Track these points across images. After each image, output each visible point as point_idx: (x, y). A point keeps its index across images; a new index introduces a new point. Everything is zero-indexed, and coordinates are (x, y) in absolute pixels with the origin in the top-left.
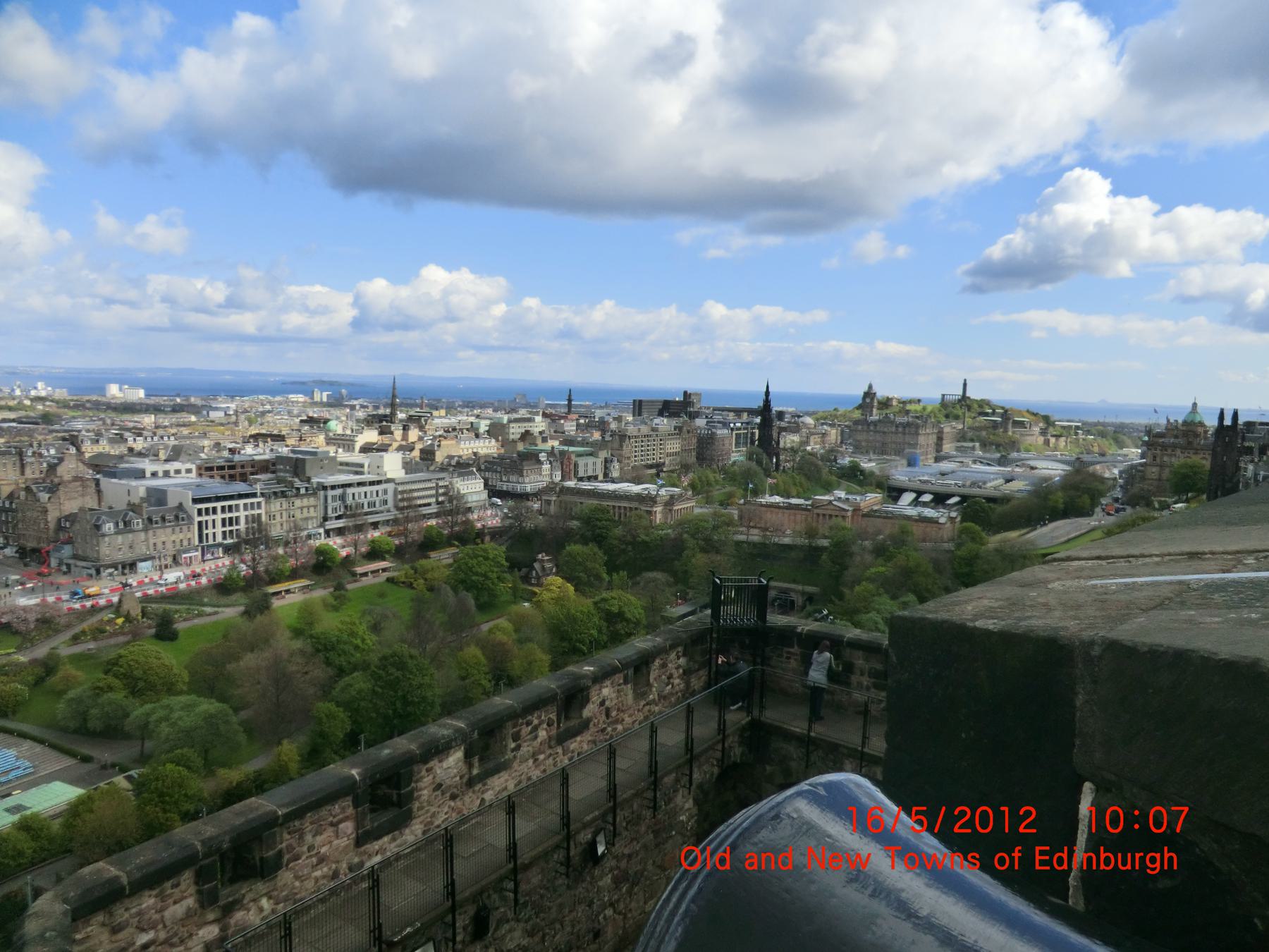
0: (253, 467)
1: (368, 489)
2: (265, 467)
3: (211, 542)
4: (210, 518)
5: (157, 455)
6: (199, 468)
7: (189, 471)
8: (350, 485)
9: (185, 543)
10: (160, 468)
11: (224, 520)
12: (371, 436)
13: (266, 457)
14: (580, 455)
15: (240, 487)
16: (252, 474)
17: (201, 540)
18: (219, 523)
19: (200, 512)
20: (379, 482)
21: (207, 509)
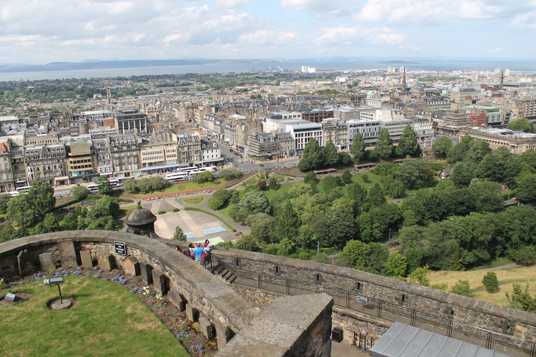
0: (326, 114)
1: (371, 127)
2: (331, 114)
3: (301, 148)
4: (301, 138)
5: (290, 108)
6: (303, 115)
7: (299, 116)
8: (362, 125)
9: (290, 148)
10: (288, 114)
11: (306, 139)
12: (387, 99)
13: (331, 110)
14: (489, 111)
15: (314, 125)
16: (325, 118)
17: (296, 148)
18: (304, 140)
19: (296, 135)
20: (378, 124)
21: (299, 134)
